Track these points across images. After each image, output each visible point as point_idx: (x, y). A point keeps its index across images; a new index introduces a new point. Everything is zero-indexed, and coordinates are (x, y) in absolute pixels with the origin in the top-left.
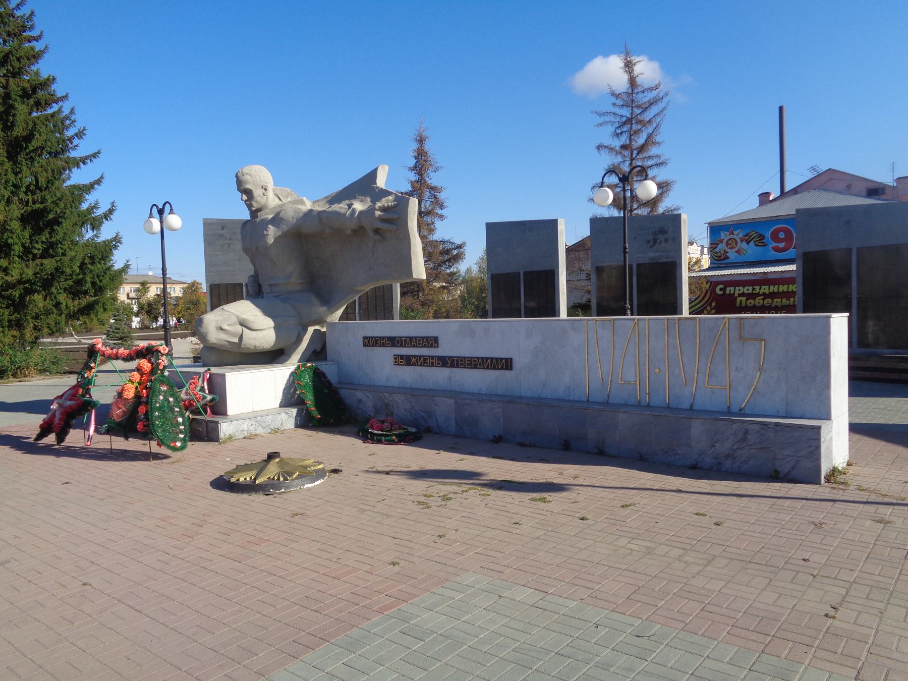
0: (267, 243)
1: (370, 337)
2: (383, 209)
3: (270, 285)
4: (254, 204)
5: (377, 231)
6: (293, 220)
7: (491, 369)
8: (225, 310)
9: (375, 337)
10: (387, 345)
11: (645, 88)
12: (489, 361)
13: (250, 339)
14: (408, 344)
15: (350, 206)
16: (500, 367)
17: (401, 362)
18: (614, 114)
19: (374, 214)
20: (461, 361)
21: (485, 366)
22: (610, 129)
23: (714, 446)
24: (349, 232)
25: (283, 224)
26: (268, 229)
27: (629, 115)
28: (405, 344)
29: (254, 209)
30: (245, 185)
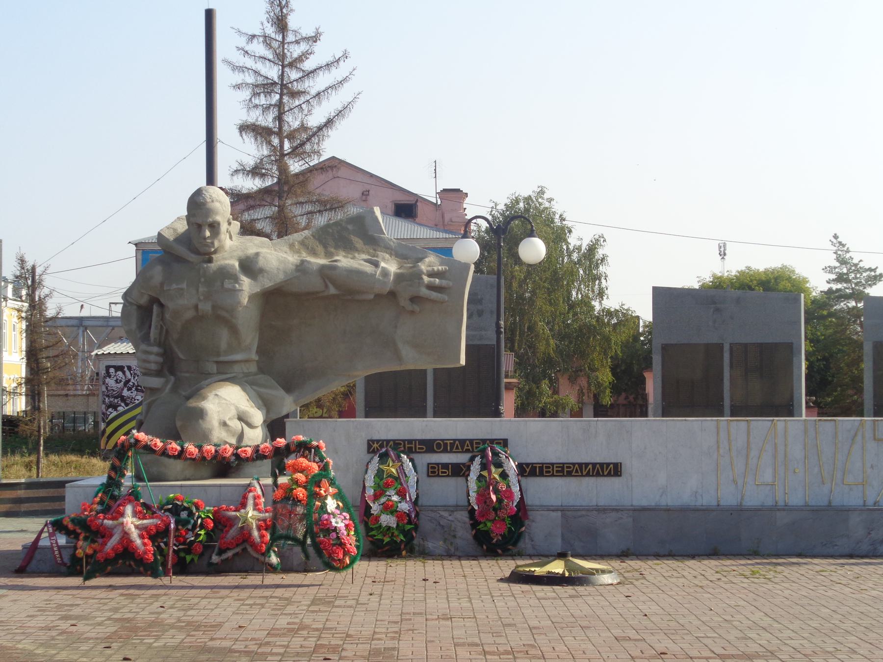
0: (239, 303)
1: (383, 441)
2: (431, 275)
3: (217, 362)
4: (216, 244)
5: (415, 299)
6: (278, 273)
7: (593, 476)
8: (221, 397)
9: (394, 441)
10: (417, 450)
11: (304, 35)
12: (590, 466)
13: (250, 439)
14: (457, 448)
15: (376, 264)
16: (606, 473)
17: (442, 472)
18: (255, 72)
19: (422, 279)
20: (548, 467)
21: (584, 473)
22: (246, 94)
23: (869, 533)
24: (371, 297)
25: (263, 277)
26: (241, 282)
27: (276, 79)
28: (452, 448)
29: (213, 250)
30: (214, 216)
